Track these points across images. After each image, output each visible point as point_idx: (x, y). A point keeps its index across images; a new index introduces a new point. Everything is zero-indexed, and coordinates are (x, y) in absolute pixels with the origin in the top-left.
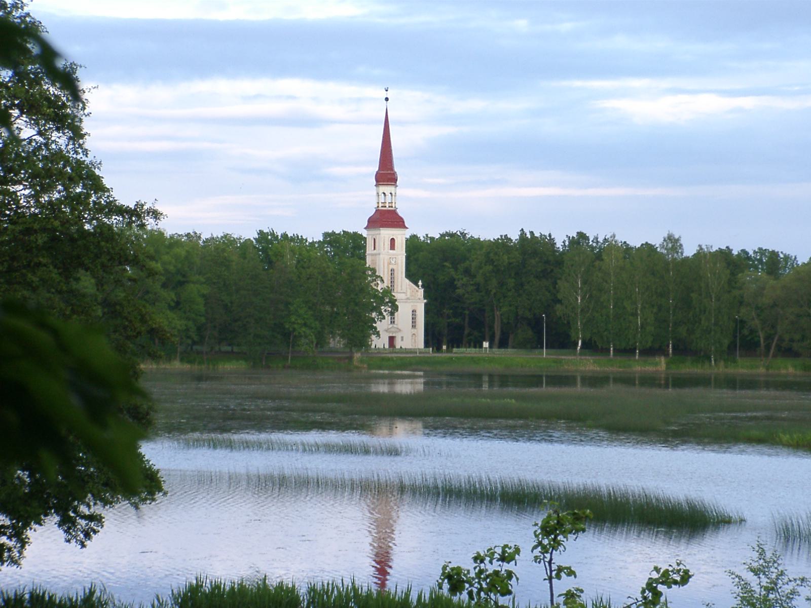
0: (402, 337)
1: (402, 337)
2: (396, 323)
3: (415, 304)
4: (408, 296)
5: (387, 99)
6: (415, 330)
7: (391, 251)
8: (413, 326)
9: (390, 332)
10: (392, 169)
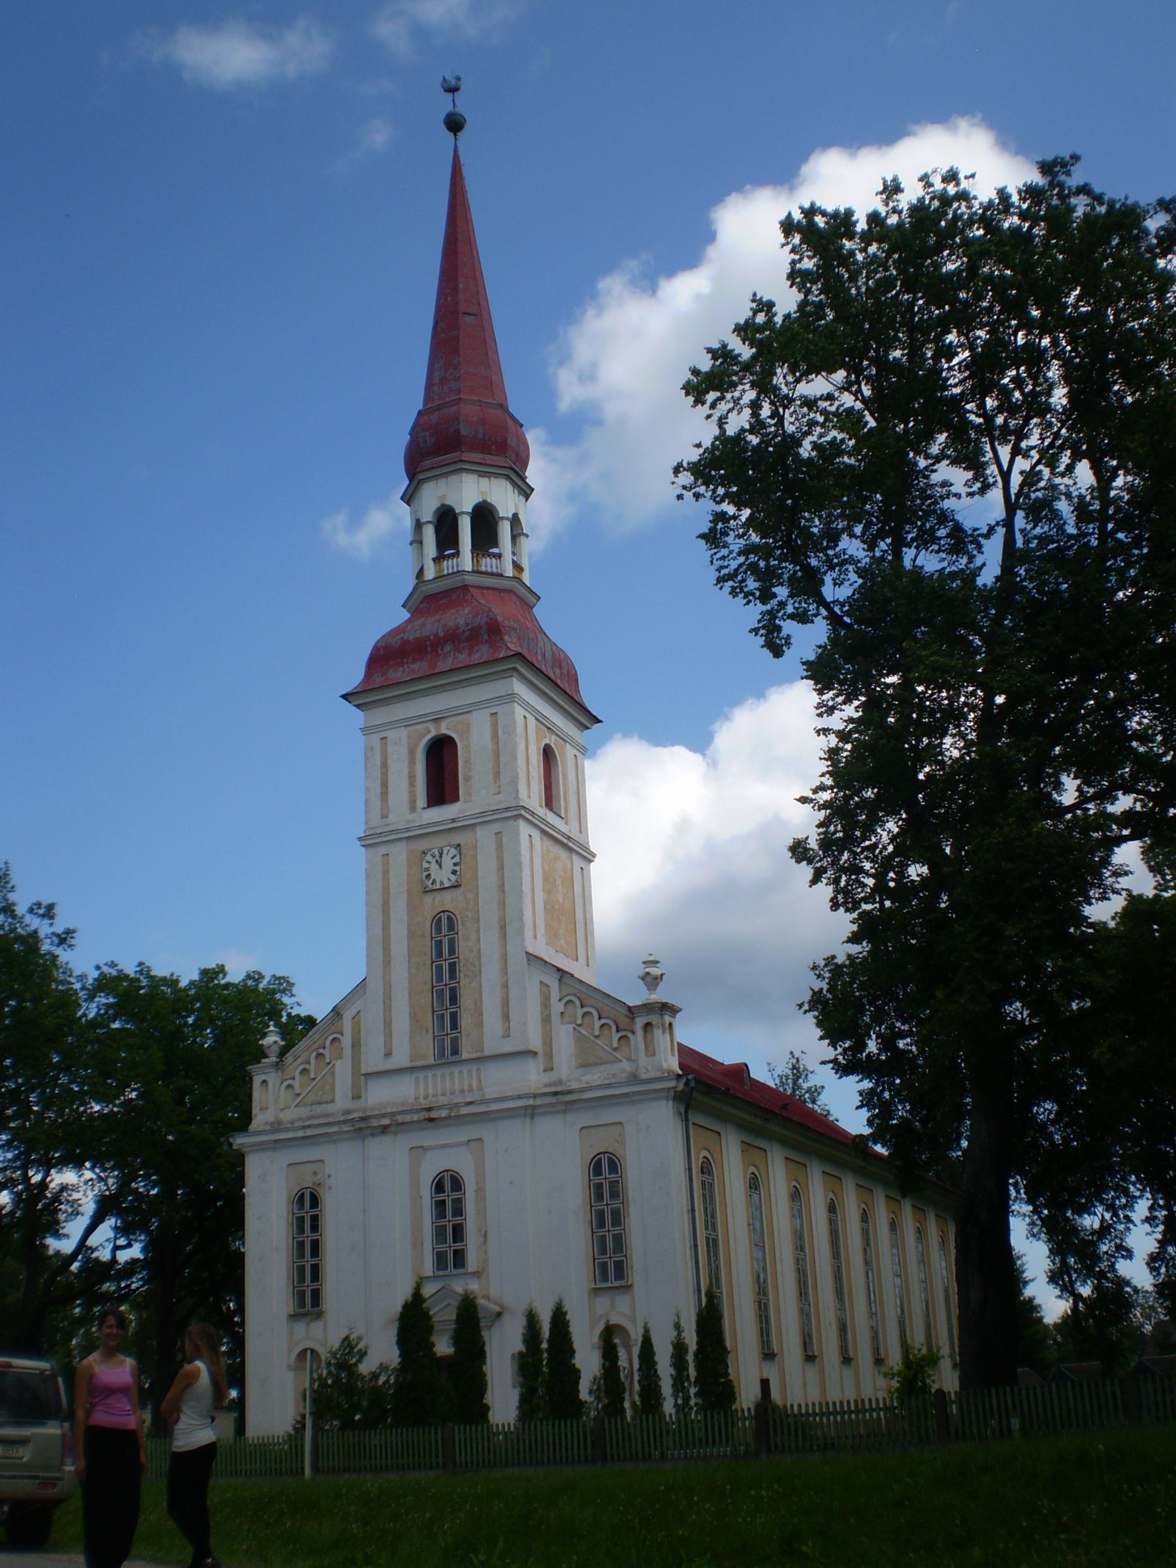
2: (472, 1260)
3: (608, 1116)
4: (566, 1068)
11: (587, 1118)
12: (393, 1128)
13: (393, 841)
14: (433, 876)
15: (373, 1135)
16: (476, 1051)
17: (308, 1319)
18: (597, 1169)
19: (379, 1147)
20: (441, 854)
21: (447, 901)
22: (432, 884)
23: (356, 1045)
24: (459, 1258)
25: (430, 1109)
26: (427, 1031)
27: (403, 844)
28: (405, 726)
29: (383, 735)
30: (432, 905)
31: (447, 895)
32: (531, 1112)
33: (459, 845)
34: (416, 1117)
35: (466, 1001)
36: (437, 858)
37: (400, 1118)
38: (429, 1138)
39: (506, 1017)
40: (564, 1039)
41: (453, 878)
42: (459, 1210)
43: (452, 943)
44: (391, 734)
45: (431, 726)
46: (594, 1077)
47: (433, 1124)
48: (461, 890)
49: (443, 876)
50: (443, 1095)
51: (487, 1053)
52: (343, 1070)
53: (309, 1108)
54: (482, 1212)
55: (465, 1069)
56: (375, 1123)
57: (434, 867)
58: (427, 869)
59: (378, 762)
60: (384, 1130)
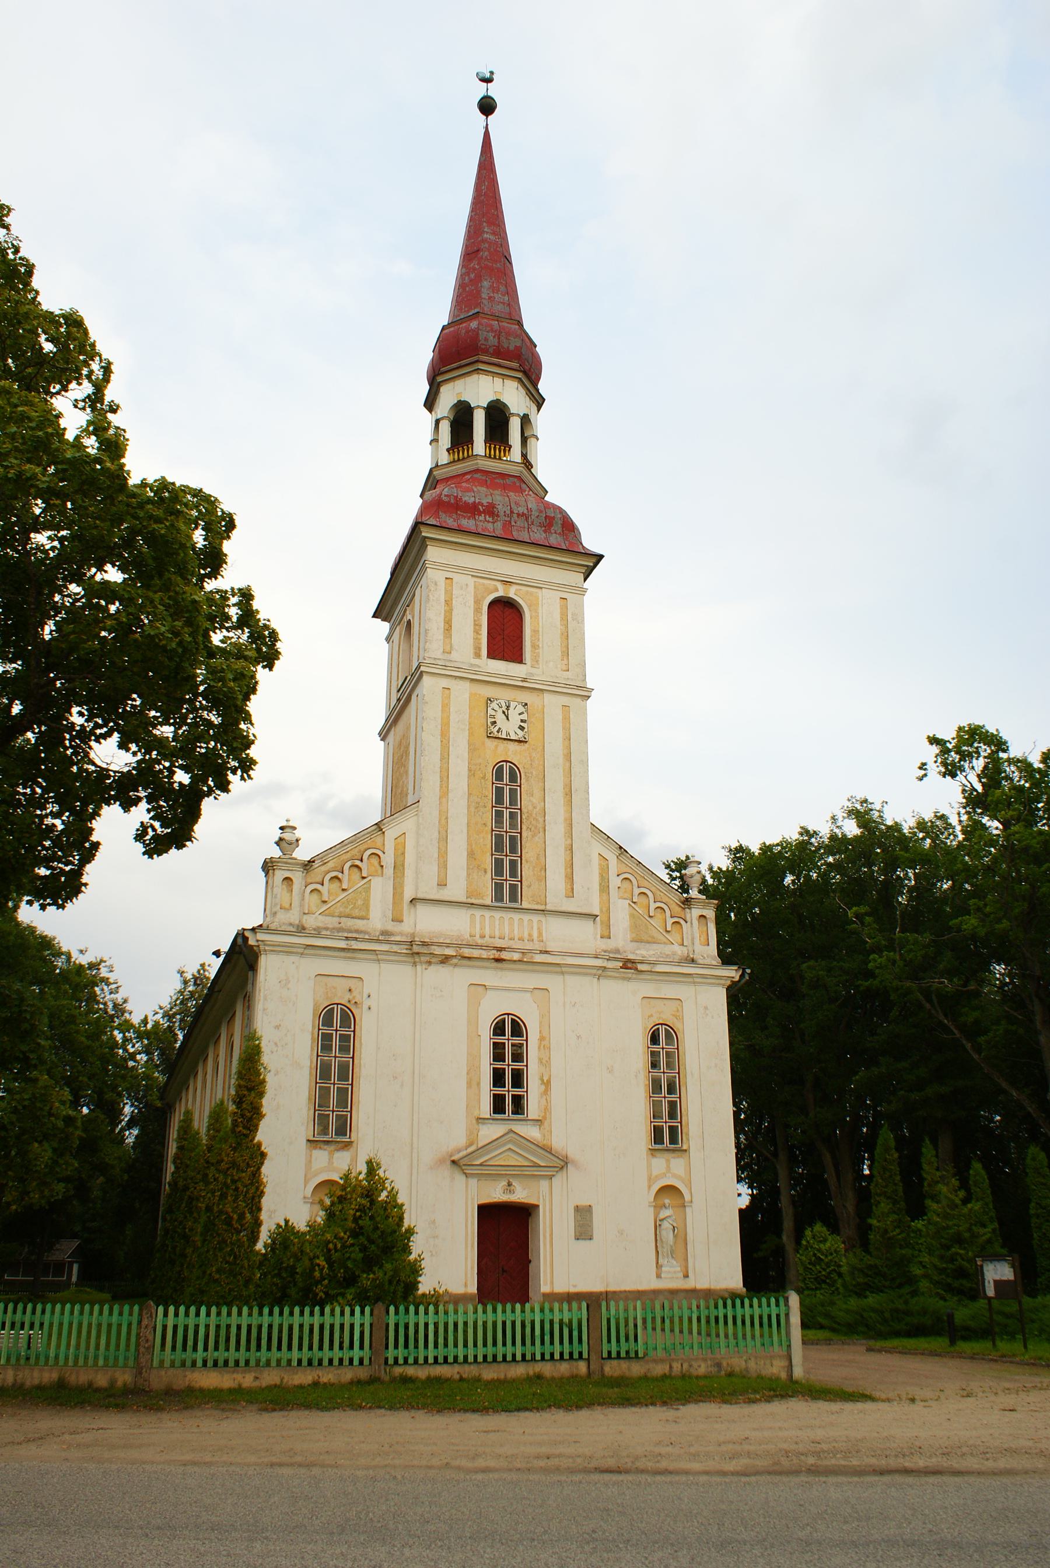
0: (583, 1216)
1: (583, 1216)
2: (533, 1106)
3: (670, 990)
4: (621, 939)
5: (487, 107)
6: (677, 1164)
7: (500, 667)
8: (657, 1135)
9: (487, 1173)
11: (648, 988)
12: (455, 961)
13: (456, 677)
14: (499, 725)
15: (430, 963)
16: (538, 903)
17: (332, 1147)
18: (654, 1039)
19: (437, 974)
20: (508, 708)
21: (513, 753)
22: (498, 732)
23: (399, 867)
24: (519, 1105)
25: (500, 949)
26: (485, 872)
27: (467, 684)
28: (472, 576)
29: (449, 575)
30: (495, 753)
31: (513, 746)
32: (601, 973)
33: (526, 704)
34: (484, 954)
35: (529, 850)
36: (504, 708)
37: (467, 952)
38: (490, 976)
39: (570, 878)
40: (621, 914)
41: (521, 733)
42: (517, 1057)
43: (513, 792)
44: (457, 578)
45: (499, 585)
47: (499, 965)
48: (526, 745)
50: (521, 939)
51: (548, 907)
53: (337, 919)
55: (526, 917)
56: (438, 951)
57: (500, 718)
58: (493, 717)
59: (442, 599)
60: (445, 960)
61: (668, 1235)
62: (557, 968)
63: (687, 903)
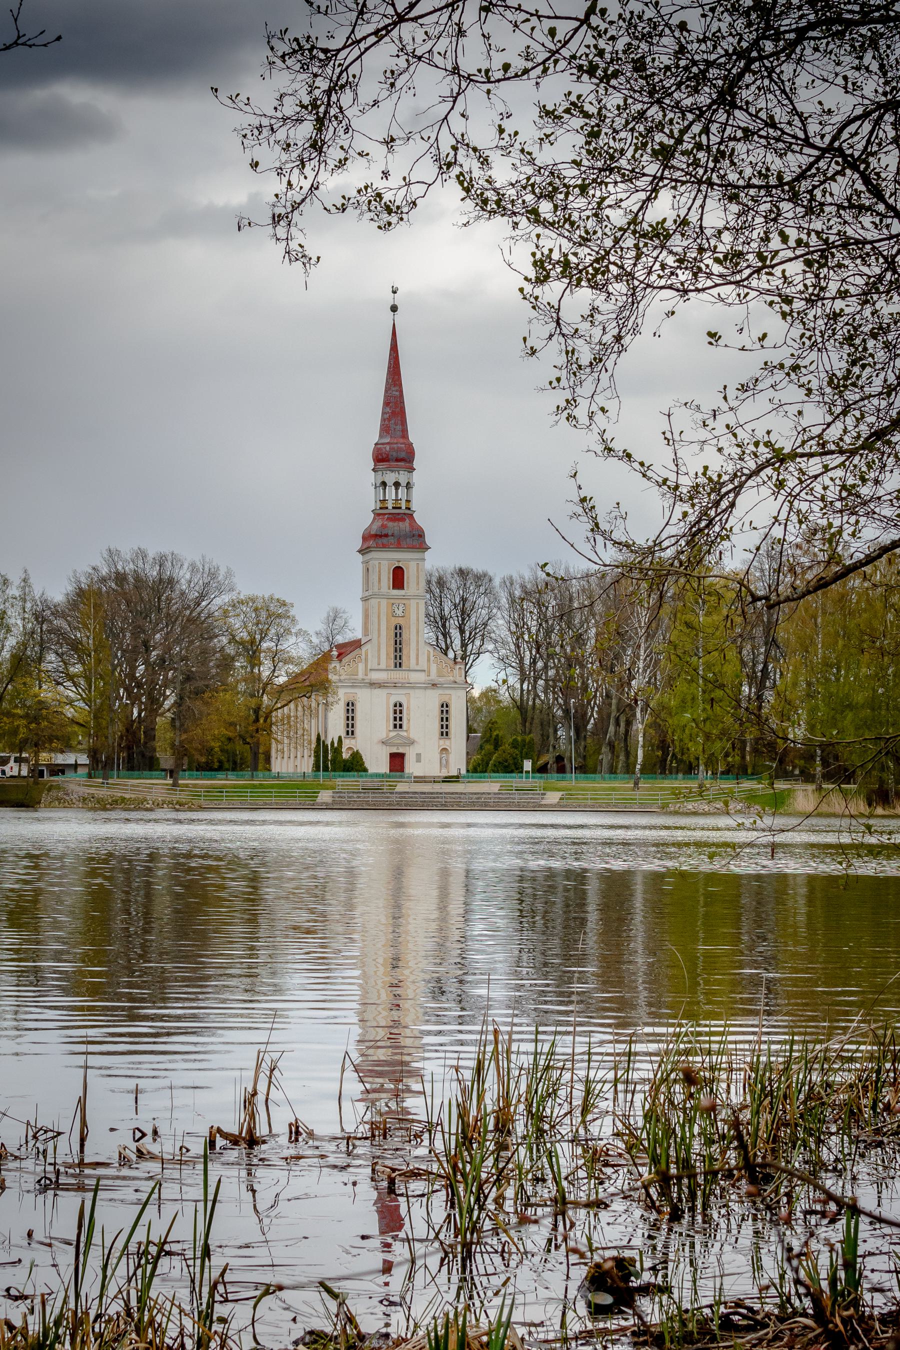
0: (419, 756)
1: (419, 756)
2: (405, 727)
5: (394, 309)
6: (447, 742)
8: (442, 734)
10: (404, 433)
11: (440, 692)
19: (377, 691)
21: (401, 621)
23: (366, 659)
24: (401, 726)
30: (395, 621)
32: (426, 688)
35: (405, 652)
38: (393, 691)
46: (441, 680)
49: (399, 612)
52: (361, 667)
54: (408, 714)
61: (444, 762)
62: (413, 688)
63: (456, 663)
